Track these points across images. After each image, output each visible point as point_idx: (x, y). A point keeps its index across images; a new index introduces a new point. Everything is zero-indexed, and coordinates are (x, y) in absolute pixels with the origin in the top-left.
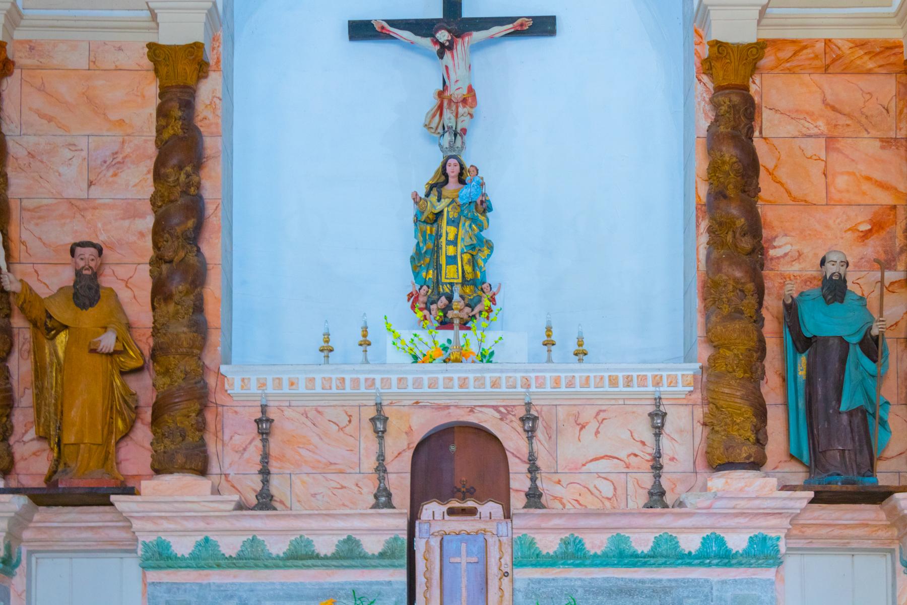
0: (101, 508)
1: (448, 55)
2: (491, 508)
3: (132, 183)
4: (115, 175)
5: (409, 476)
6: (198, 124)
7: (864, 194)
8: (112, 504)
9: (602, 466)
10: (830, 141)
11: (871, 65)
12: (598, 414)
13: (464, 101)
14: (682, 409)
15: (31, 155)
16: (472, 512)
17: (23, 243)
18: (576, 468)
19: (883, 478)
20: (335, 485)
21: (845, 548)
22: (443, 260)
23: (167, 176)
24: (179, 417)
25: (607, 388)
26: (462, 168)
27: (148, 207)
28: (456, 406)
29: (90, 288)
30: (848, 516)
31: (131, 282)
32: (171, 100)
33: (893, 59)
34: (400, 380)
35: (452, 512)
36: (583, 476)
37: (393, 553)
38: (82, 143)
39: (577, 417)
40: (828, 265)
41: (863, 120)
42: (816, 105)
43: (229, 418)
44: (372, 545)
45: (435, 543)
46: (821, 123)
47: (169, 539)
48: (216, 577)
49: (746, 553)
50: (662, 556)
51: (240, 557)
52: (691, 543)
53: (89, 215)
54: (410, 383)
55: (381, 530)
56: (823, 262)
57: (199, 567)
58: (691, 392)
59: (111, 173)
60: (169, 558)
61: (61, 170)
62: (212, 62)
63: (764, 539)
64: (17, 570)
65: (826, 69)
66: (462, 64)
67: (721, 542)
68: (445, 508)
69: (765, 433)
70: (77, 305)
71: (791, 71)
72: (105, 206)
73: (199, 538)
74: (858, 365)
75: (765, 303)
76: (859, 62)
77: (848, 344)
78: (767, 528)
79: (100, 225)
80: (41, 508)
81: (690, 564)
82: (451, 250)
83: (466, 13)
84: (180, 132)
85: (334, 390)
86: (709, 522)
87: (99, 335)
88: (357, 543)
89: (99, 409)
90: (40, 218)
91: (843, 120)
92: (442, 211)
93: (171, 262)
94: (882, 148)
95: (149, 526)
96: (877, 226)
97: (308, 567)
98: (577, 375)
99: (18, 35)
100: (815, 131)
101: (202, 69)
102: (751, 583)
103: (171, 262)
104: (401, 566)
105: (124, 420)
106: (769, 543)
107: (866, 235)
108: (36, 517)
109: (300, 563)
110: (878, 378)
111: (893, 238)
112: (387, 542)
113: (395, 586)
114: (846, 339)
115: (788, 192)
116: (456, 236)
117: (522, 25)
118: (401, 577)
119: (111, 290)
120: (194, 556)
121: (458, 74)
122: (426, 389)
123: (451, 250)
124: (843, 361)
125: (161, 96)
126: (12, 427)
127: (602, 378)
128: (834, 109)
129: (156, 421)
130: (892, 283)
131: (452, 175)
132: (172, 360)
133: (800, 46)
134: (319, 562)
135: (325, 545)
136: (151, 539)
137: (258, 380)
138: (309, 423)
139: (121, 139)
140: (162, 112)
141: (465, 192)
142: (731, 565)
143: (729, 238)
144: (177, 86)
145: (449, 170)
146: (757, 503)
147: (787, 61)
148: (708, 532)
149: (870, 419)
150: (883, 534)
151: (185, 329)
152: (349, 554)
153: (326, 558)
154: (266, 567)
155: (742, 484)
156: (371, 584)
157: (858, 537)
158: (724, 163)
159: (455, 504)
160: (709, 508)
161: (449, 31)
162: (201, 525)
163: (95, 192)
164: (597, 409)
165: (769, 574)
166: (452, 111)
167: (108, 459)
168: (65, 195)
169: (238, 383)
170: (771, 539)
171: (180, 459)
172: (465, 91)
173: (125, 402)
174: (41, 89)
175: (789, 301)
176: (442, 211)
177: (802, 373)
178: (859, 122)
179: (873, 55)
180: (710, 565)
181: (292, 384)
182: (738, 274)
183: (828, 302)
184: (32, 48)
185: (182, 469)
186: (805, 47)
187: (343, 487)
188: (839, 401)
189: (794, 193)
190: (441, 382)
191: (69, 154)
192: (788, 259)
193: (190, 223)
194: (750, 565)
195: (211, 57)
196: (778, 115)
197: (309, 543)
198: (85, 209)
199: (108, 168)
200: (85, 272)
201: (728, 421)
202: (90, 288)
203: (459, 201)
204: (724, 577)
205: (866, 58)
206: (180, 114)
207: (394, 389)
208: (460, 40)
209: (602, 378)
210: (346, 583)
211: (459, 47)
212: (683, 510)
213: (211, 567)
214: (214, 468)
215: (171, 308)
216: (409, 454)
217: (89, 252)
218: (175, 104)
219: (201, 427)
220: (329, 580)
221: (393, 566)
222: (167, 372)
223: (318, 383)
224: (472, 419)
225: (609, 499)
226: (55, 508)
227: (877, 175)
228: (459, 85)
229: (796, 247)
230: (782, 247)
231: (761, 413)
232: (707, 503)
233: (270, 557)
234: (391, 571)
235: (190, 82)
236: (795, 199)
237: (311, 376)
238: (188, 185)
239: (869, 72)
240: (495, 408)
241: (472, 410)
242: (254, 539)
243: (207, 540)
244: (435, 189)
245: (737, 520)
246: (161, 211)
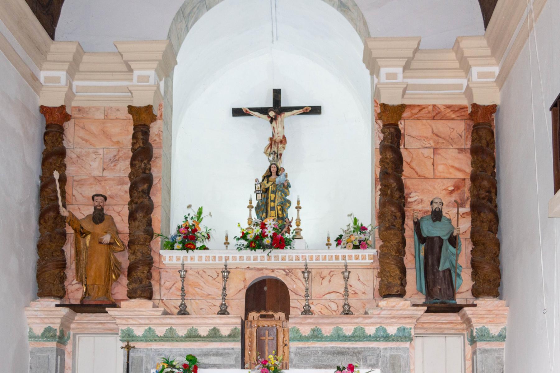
0: (102, 314)
1: (274, 122)
2: (282, 315)
3: (122, 169)
4: (115, 166)
5: (244, 300)
6: (152, 143)
7: (451, 173)
8: (107, 312)
9: (333, 296)
10: (435, 150)
11: (453, 116)
12: (330, 273)
13: (281, 142)
14: (368, 270)
15: (78, 157)
16: (272, 316)
17: (74, 196)
18: (320, 298)
19: (459, 300)
20: (211, 304)
21: (442, 333)
22: (269, 210)
23: (135, 165)
24: (140, 273)
25: (334, 261)
26: (278, 168)
27: (128, 180)
28: (266, 269)
29: (100, 215)
30: (443, 319)
31: (119, 213)
32: (138, 131)
33: (463, 113)
34: (240, 257)
35: (262, 316)
36: (323, 301)
37: (234, 335)
38: (101, 151)
39: (321, 274)
40: (434, 204)
41: (450, 140)
42: (429, 134)
43: (163, 274)
44: (225, 331)
45: (254, 330)
46: (431, 142)
47: (133, 328)
48: (155, 346)
49: (396, 336)
50: (357, 336)
51: (165, 336)
52: (371, 330)
53: (103, 183)
54: (245, 258)
55: (229, 324)
56: (432, 203)
57: (147, 341)
58: (372, 263)
59: (113, 164)
60: (133, 336)
61: (91, 163)
62: (158, 116)
63: (404, 329)
64: (68, 342)
65: (433, 118)
66: (280, 126)
67: (385, 330)
68: (258, 315)
69: (406, 281)
70: (94, 222)
71: (418, 119)
72: (110, 179)
73: (147, 328)
74: (447, 249)
75: (406, 222)
76: (448, 115)
77: (443, 240)
78: (405, 323)
79: (107, 188)
80: (78, 314)
81: (370, 340)
82: (272, 204)
83: (283, 104)
84: (142, 145)
85: (211, 262)
86: (379, 321)
87: (103, 235)
88: (218, 330)
89: (103, 269)
90: (81, 185)
91: (441, 140)
92: (269, 188)
93: (136, 203)
94: (459, 153)
95: (124, 322)
96: (457, 188)
97: (196, 341)
98: (321, 255)
99: (74, 104)
100: (428, 145)
101: (154, 118)
102: (398, 349)
103: (136, 203)
104: (238, 341)
105: (115, 275)
106: (406, 331)
107: (452, 192)
108: (76, 318)
109: (192, 339)
110: (457, 255)
111: (464, 193)
112: (232, 330)
113: (236, 350)
114: (443, 238)
115: (417, 173)
116: (275, 198)
117: (306, 110)
118: (238, 346)
119: (110, 216)
120: (144, 336)
121: (279, 129)
122: (252, 261)
123: (272, 204)
124: (441, 248)
125: (134, 129)
126: (66, 277)
127: (332, 256)
128: (437, 135)
129: (129, 275)
130: (463, 214)
131: (273, 172)
132: (136, 247)
133: (422, 108)
134: (201, 339)
135: (203, 331)
136: (125, 328)
137: (177, 257)
138: (200, 277)
139: (117, 150)
140: (134, 137)
141: (279, 180)
142: (389, 341)
143: (389, 192)
144: (141, 125)
145: (272, 169)
146: (401, 312)
147: (416, 114)
148: (378, 326)
149: (453, 275)
150: (459, 327)
151: (142, 233)
152: (214, 335)
153: (204, 337)
154: (177, 341)
155: (393, 304)
156: (224, 349)
157: (448, 329)
158: (387, 158)
159: (263, 313)
160: (379, 314)
161: (275, 112)
162: (147, 322)
163: (106, 173)
164: (329, 270)
165: (407, 345)
166: (276, 146)
167: (107, 291)
168: (93, 175)
169: (167, 259)
170: (407, 329)
171: (139, 292)
172: (281, 138)
173: (116, 266)
174: (83, 128)
175: (416, 220)
176: (269, 188)
177: (422, 254)
178: (448, 141)
179: (454, 111)
180: (379, 341)
181: (192, 259)
182: (393, 209)
183: (434, 221)
184: (79, 110)
185: (140, 297)
186: (424, 108)
187: (214, 305)
188: (439, 266)
189: (419, 173)
190: (259, 258)
191: (94, 156)
192: (416, 203)
193: (146, 186)
194: (398, 341)
195: (156, 112)
196: (412, 139)
197: (196, 330)
198: (102, 181)
199: (112, 162)
200: (98, 208)
201: (388, 274)
202: (100, 215)
203: (277, 183)
204: (385, 347)
205: (451, 113)
206: (142, 137)
207: (238, 261)
208: (279, 116)
209: (332, 256)
210: (213, 349)
211: (279, 119)
212: (367, 315)
213: (152, 341)
214: (156, 296)
215: (137, 224)
216: (245, 291)
217: (100, 199)
218: (140, 134)
219: (149, 277)
220: (206, 347)
221: (234, 341)
222: (134, 253)
223: (204, 259)
224: (273, 275)
225: (335, 311)
226: (84, 314)
227: (457, 165)
228: (279, 135)
229: (420, 197)
230: (413, 197)
231: (403, 271)
232: (378, 312)
233: (178, 336)
234: (234, 343)
235: (147, 123)
236: (419, 176)
237: (201, 255)
238: (145, 169)
239: (453, 119)
240: (284, 270)
241: (273, 271)
242: (171, 328)
243: (150, 328)
244: (266, 179)
245: (392, 320)
246: (133, 181)
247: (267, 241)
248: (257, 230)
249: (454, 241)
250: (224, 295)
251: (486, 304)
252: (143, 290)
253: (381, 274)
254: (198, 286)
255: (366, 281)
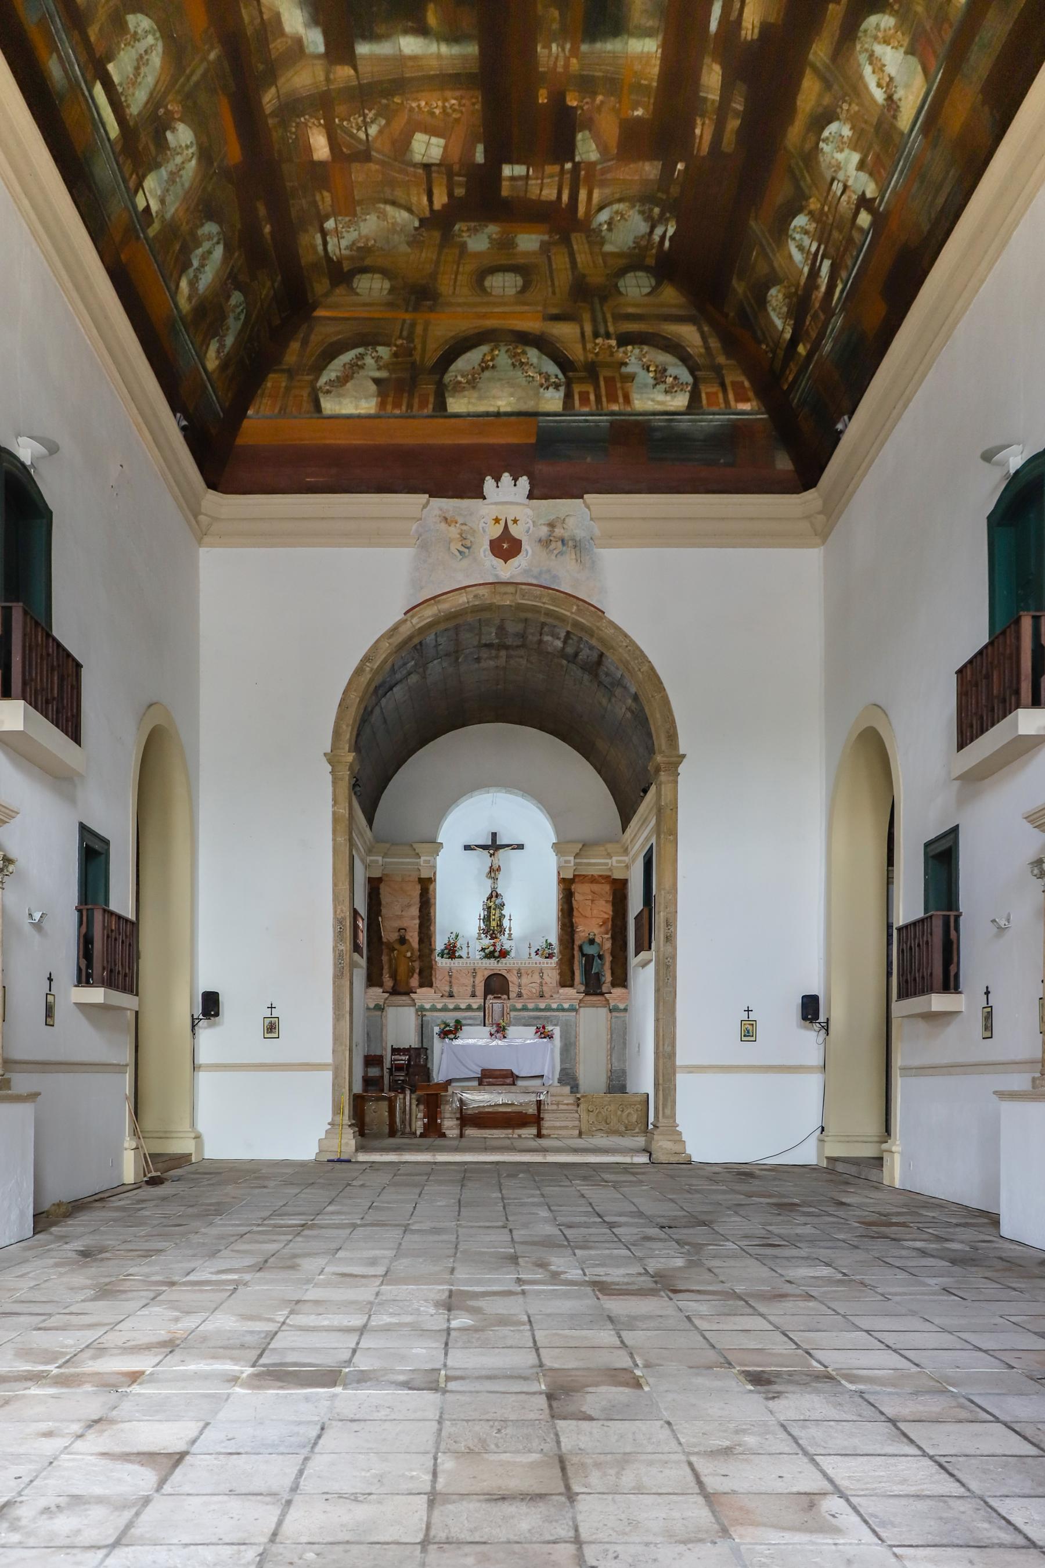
2: (505, 996)
19: (604, 989)
44: (475, 1006)
52: (554, 1006)
110: (603, 965)
135: (463, 1006)
152: (469, 1008)
219: (431, 975)
231: (573, 973)
247: (497, 954)
248: (492, 948)
249: (600, 957)
250: (474, 986)
251: (618, 991)
252: (427, 982)
253: (560, 974)
254: (457, 979)
255: (552, 976)
